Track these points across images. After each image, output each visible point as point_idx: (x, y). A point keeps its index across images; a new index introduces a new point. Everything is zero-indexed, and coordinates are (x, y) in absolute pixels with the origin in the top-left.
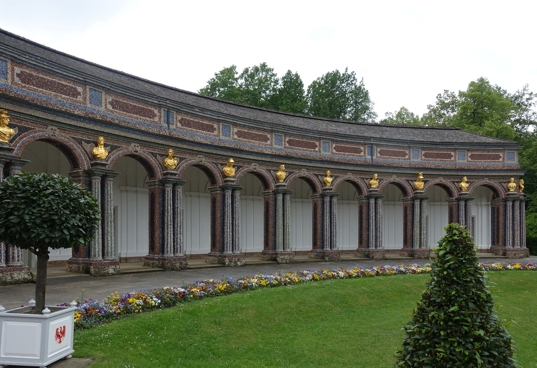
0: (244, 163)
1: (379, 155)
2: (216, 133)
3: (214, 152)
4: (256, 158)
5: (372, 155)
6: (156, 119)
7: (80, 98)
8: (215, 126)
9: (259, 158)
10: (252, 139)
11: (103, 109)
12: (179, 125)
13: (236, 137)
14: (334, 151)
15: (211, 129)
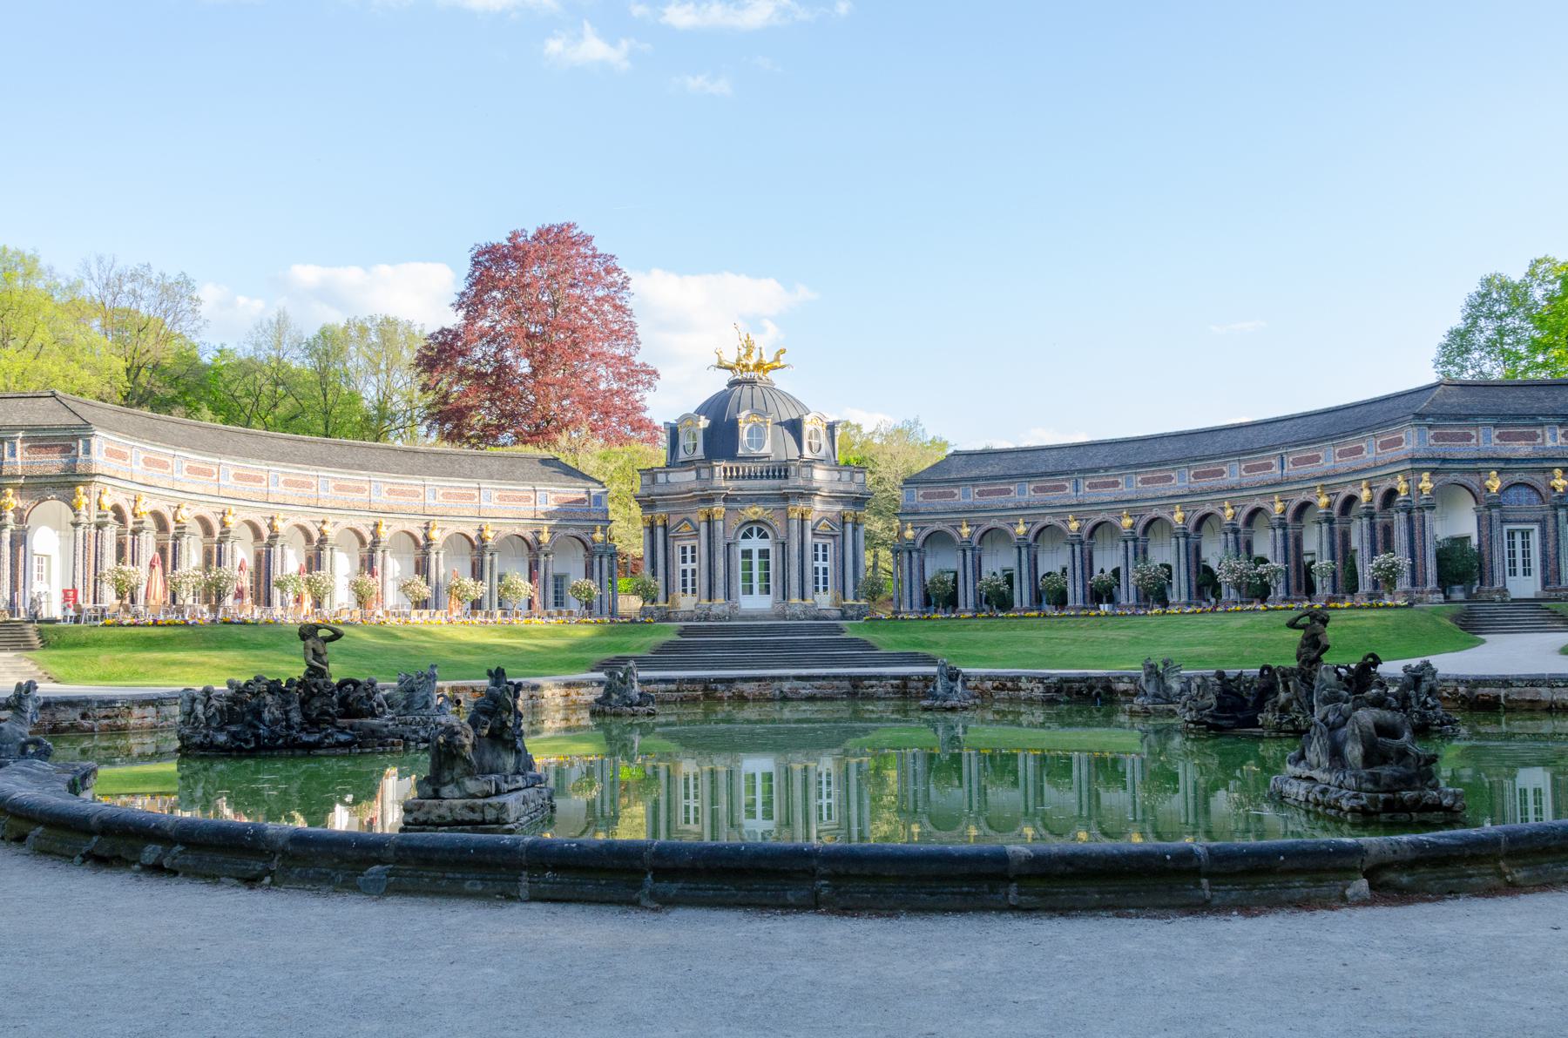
0: (1146, 511)
1: (1291, 466)
2: (1120, 486)
3: (1112, 507)
4: (1153, 503)
5: (1283, 468)
6: (1067, 491)
7: (1012, 494)
8: (1120, 480)
9: (1157, 503)
10: (1156, 482)
11: (1027, 496)
12: (1087, 489)
13: (1140, 485)
14: (1244, 473)
15: (1116, 484)
